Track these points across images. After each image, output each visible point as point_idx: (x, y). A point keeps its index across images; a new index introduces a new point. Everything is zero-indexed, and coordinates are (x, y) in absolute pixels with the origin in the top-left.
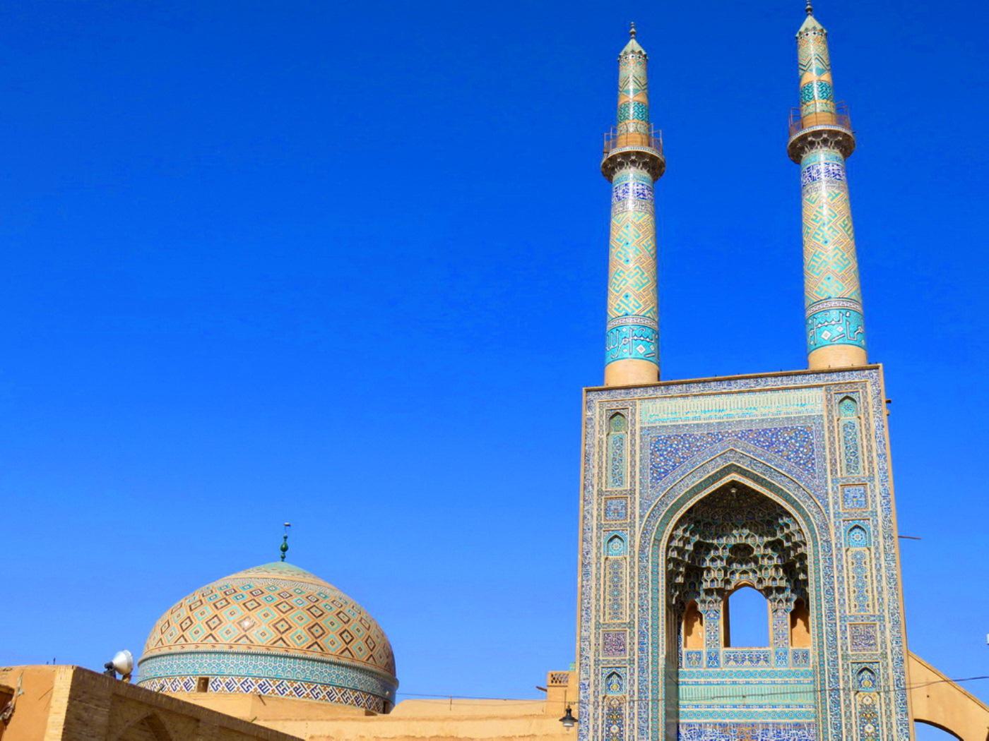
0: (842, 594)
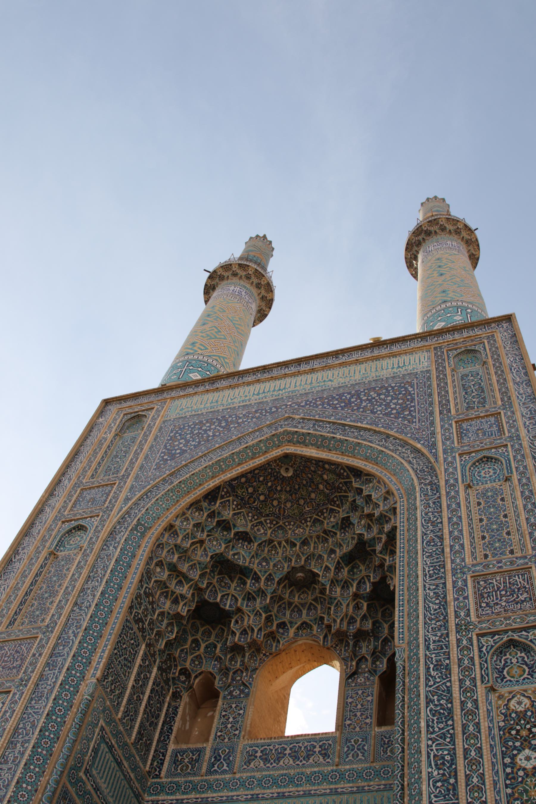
0: (456, 539)
